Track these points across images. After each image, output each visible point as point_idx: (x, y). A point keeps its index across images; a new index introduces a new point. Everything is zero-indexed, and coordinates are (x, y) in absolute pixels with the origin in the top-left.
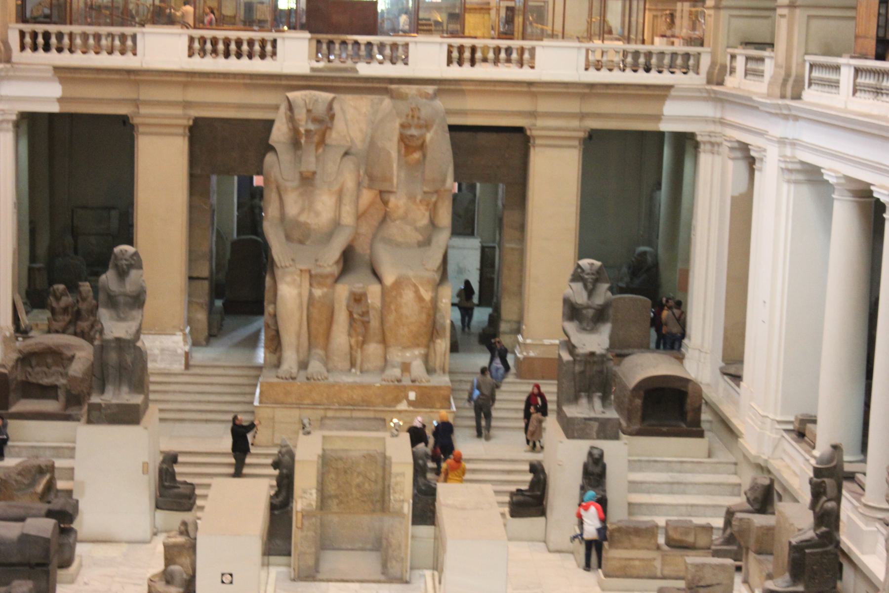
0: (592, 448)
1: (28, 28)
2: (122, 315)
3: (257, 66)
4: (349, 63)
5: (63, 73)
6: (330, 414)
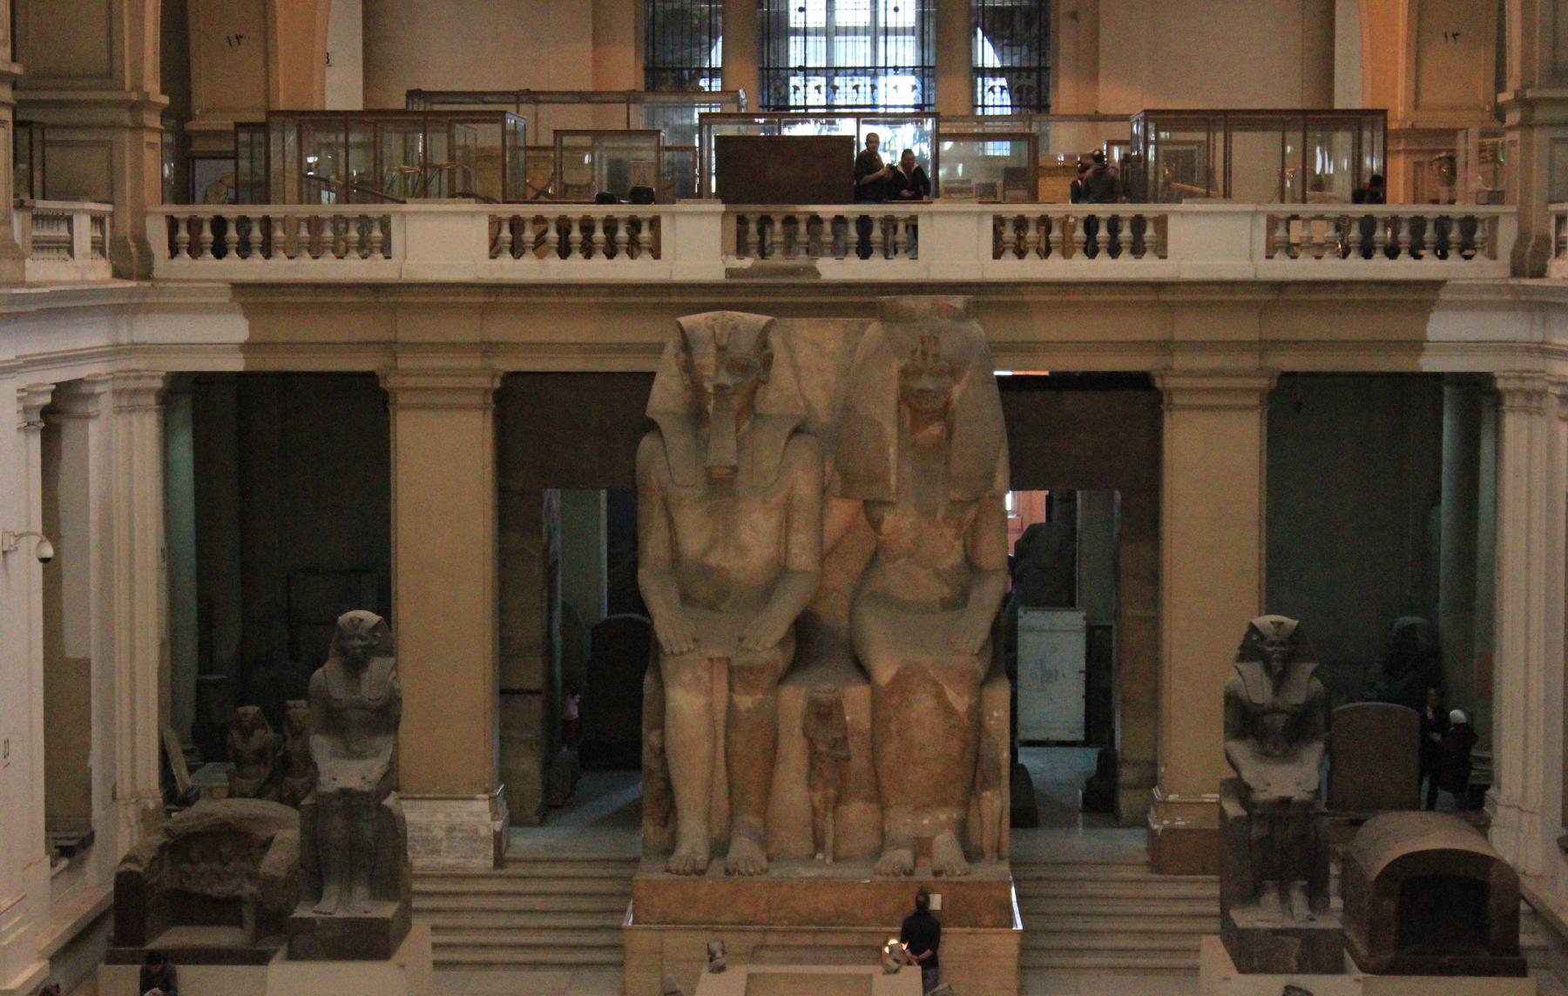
0: (1287, 988)
1: (182, 211)
2: (356, 747)
3: (626, 269)
4: (801, 259)
5: (250, 296)
6: (773, 939)
